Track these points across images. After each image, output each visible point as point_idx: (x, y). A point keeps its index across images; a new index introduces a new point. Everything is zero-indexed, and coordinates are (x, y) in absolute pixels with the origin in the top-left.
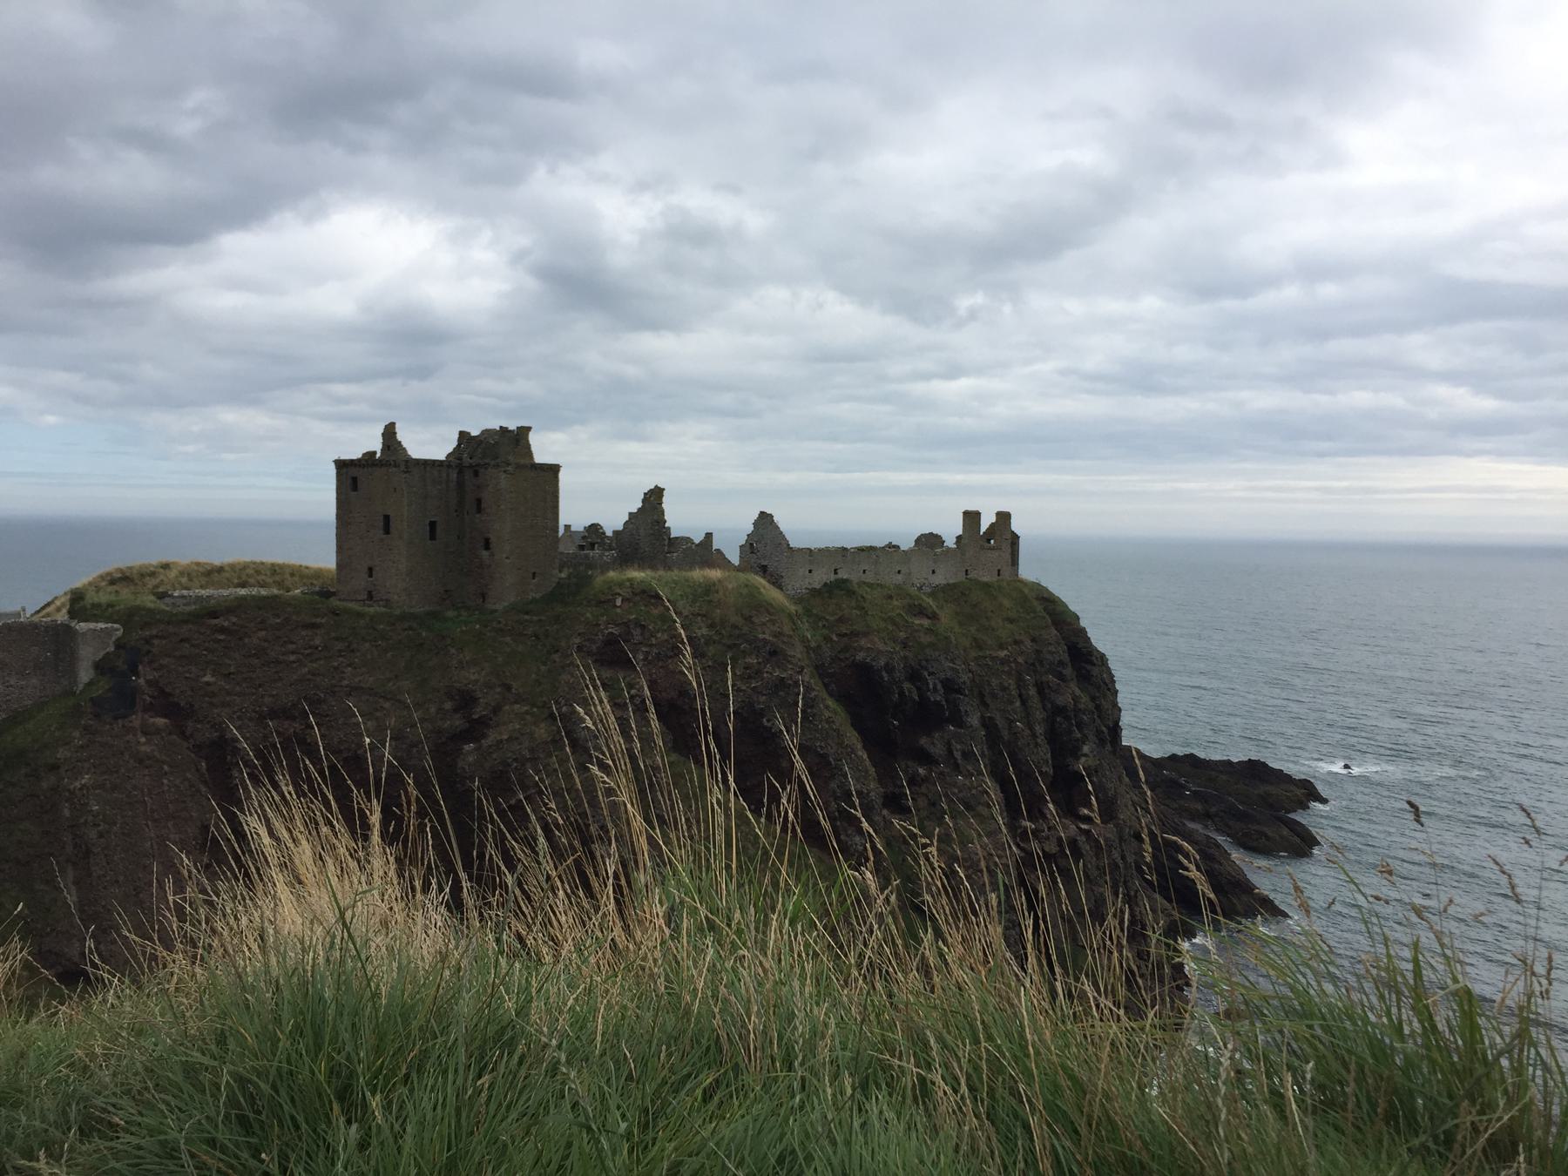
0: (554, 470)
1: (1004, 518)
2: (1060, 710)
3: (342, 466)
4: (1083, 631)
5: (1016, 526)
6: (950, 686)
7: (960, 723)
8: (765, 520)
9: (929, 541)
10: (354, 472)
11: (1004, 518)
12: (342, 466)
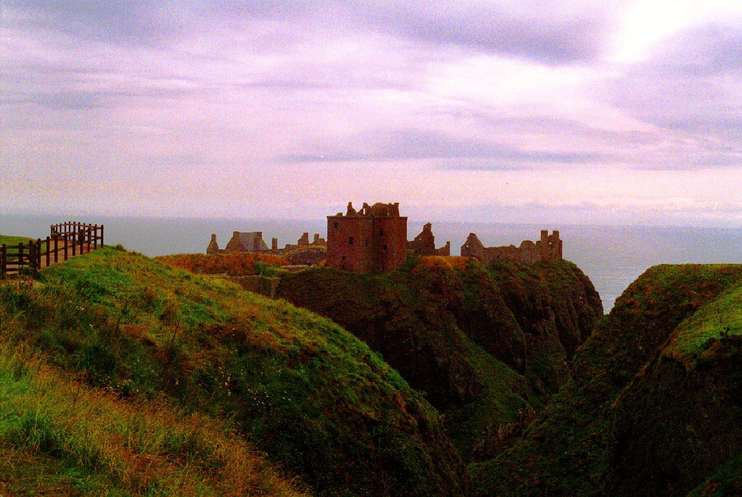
0: (406, 219)
1: (556, 233)
2: (582, 315)
3: (330, 219)
4: (590, 282)
5: (561, 237)
6: (545, 304)
7: (548, 319)
8: (472, 237)
9: (527, 244)
10: (336, 221)
11: (556, 233)
12: (330, 219)
